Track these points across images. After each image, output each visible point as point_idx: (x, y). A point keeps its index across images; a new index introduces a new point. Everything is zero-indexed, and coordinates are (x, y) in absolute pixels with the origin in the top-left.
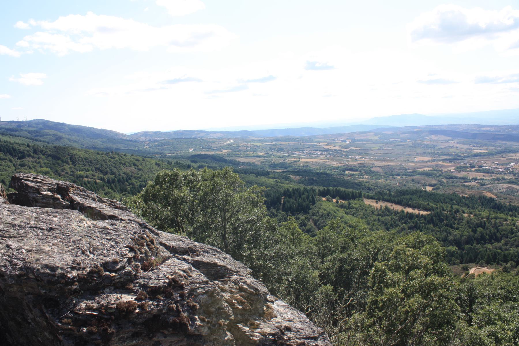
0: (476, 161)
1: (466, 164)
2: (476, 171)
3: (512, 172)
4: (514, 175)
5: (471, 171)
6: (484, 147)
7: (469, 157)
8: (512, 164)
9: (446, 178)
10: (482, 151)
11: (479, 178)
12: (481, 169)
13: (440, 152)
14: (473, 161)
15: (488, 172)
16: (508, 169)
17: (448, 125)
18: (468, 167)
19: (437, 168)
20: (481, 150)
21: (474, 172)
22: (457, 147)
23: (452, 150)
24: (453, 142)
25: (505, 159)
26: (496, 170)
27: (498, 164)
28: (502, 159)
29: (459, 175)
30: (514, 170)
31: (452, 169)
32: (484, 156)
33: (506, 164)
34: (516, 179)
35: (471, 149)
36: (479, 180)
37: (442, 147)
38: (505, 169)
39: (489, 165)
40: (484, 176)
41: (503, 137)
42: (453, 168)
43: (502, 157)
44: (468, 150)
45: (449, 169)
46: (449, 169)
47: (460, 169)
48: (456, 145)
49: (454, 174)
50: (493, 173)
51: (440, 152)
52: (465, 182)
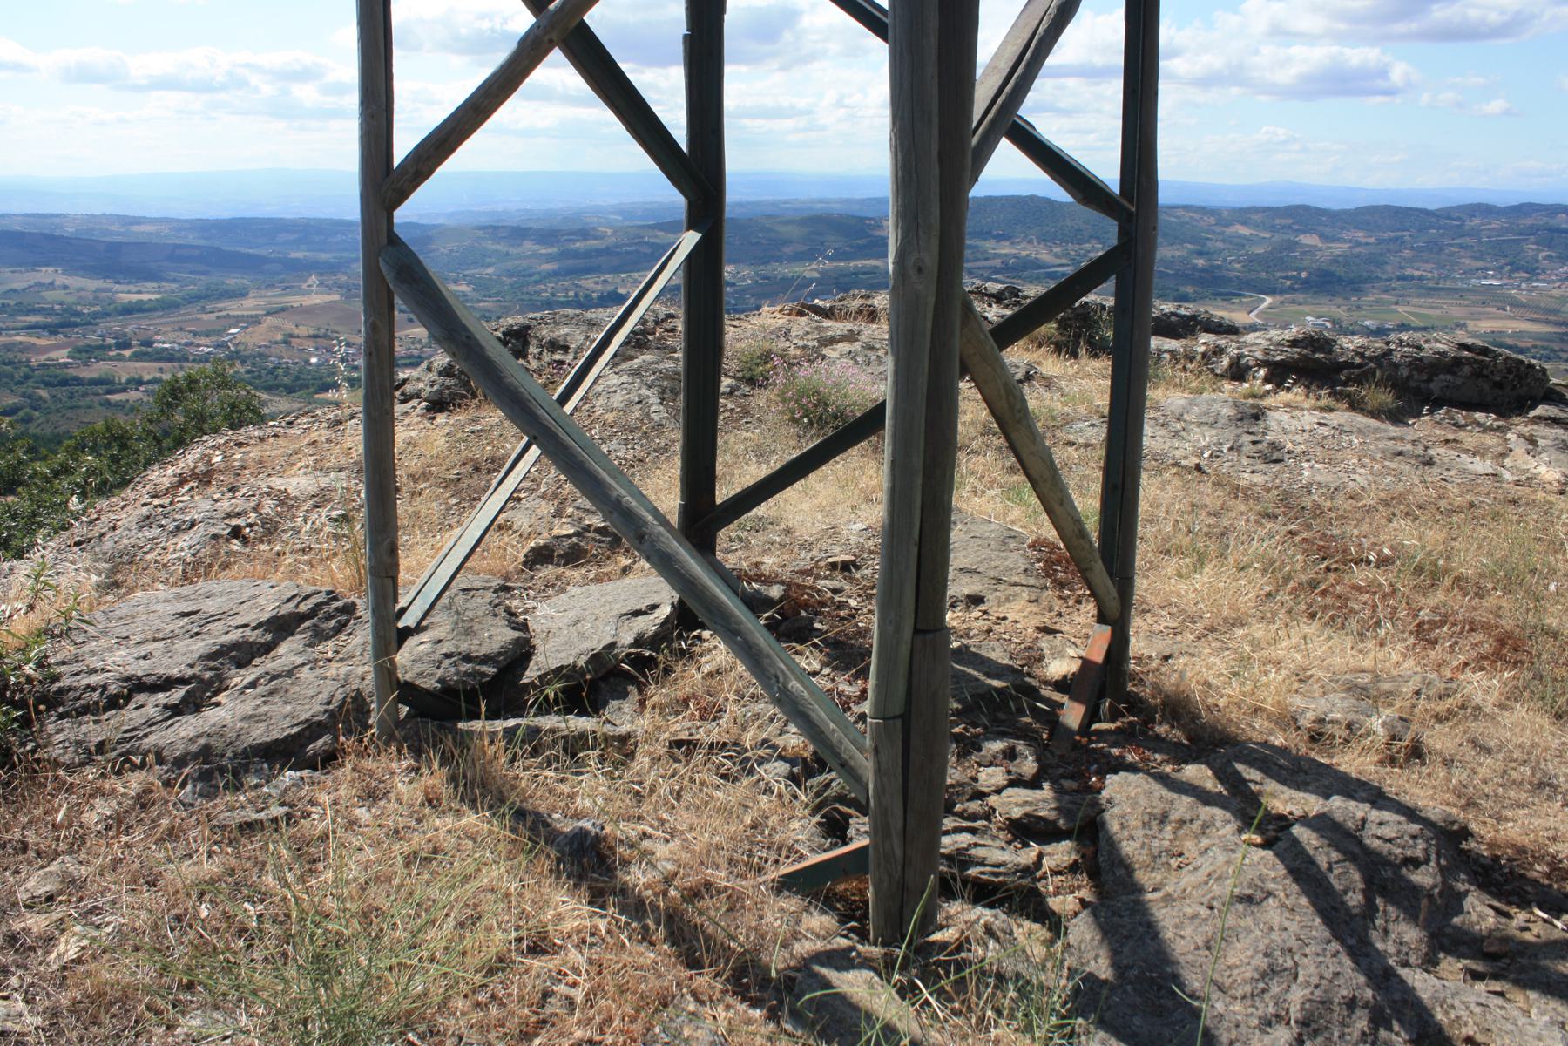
0: (131, 326)
1: (103, 337)
2: (137, 357)
3: (237, 352)
4: (243, 362)
5: (121, 358)
6: (149, 285)
7: (108, 315)
8: (233, 331)
9: (47, 384)
10: (145, 297)
11: (147, 377)
12: (148, 352)
13: (12, 303)
14: (125, 326)
15: (171, 359)
16: (224, 345)
17: (27, 215)
18: (109, 347)
19: (10, 355)
20: (139, 292)
21: (130, 359)
22: (65, 287)
23: (49, 295)
24: (51, 269)
25: (212, 317)
26: (192, 350)
27: (195, 334)
28: (205, 317)
29: (86, 374)
30: (241, 347)
31: (62, 356)
32: (150, 310)
33: (219, 333)
34: (248, 372)
35: (110, 290)
36: (149, 382)
37: (18, 286)
38: (217, 347)
39: (171, 336)
40: (161, 370)
41: (197, 252)
42: (65, 352)
43: (203, 310)
44: (103, 295)
45: (53, 355)
46: (53, 355)
47: (86, 353)
48: (61, 279)
49: (72, 372)
50: (187, 360)
51: (12, 303)
52: (109, 392)
